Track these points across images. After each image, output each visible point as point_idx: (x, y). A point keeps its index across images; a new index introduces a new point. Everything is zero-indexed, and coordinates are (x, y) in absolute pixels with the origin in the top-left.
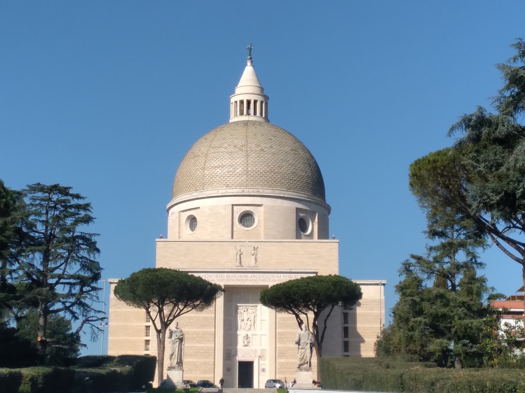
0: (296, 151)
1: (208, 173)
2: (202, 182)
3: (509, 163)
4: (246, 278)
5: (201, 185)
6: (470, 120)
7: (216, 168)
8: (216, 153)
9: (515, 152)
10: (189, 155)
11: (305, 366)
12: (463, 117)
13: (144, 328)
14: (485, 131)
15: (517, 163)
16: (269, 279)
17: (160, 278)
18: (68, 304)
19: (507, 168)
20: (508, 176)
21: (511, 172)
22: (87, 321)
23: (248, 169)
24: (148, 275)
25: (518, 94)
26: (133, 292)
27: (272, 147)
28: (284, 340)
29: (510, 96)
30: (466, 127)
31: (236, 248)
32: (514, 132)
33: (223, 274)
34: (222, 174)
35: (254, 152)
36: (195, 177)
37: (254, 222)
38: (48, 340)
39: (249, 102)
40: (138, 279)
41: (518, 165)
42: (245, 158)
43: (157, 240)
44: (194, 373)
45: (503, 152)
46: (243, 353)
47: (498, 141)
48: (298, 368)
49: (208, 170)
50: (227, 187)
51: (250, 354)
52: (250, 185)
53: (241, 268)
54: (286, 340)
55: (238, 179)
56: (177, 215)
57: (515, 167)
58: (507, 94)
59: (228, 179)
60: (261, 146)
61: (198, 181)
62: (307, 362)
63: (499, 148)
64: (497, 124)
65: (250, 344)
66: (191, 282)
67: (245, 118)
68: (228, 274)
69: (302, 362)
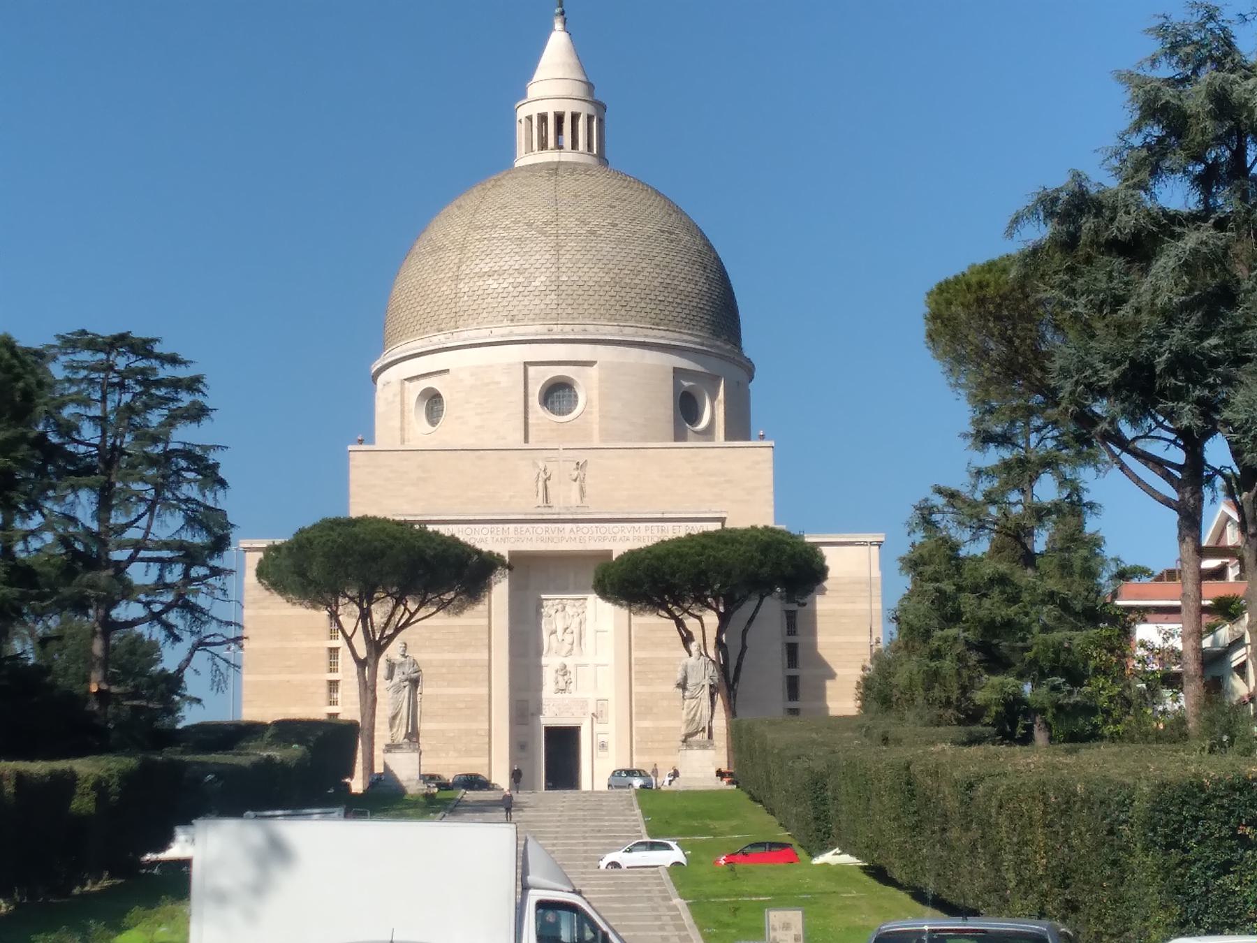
2: (454, 310)
3: (1139, 295)
4: (560, 535)
6: (1055, 200)
7: (485, 278)
8: (486, 242)
9: (1153, 271)
10: (421, 246)
11: (698, 737)
12: (1039, 194)
13: (325, 653)
14: (1088, 224)
15: (1158, 297)
16: (613, 535)
17: (363, 540)
18: (157, 608)
19: (1136, 308)
20: (1136, 326)
21: (1145, 317)
22: (201, 645)
23: (560, 279)
24: (334, 535)
25: (1160, 140)
26: (303, 574)
28: (650, 676)
29: (1143, 147)
30: (1046, 217)
31: (535, 465)
32: (1152, 227)
34: (500, 290)
35: (573, 237)
36: (435, 300)
37: (576, 402)
38: (114, 689)
39: (559, 118)
40: (311, 544)
41: (1158, 302)
42: (552, 252)
43: (350, 448)
45: (1127, 274)
46: (554, 708)
47: (1116, 247)
49: (466, 281)
50: (512, 320)
52: (564, 315)
53: (549, 510)
55: (537, 302)
56: (396, 388)
57: (1153, 304)
58: (1137, 141)
59: (515, 303)
62: (704, 728)
63: (1118, 263)
64: (1114, 209)
65: (572, 687)
66: (435, 549)
67: (550, 156)
68: (519, 526)
69: (692, 728)
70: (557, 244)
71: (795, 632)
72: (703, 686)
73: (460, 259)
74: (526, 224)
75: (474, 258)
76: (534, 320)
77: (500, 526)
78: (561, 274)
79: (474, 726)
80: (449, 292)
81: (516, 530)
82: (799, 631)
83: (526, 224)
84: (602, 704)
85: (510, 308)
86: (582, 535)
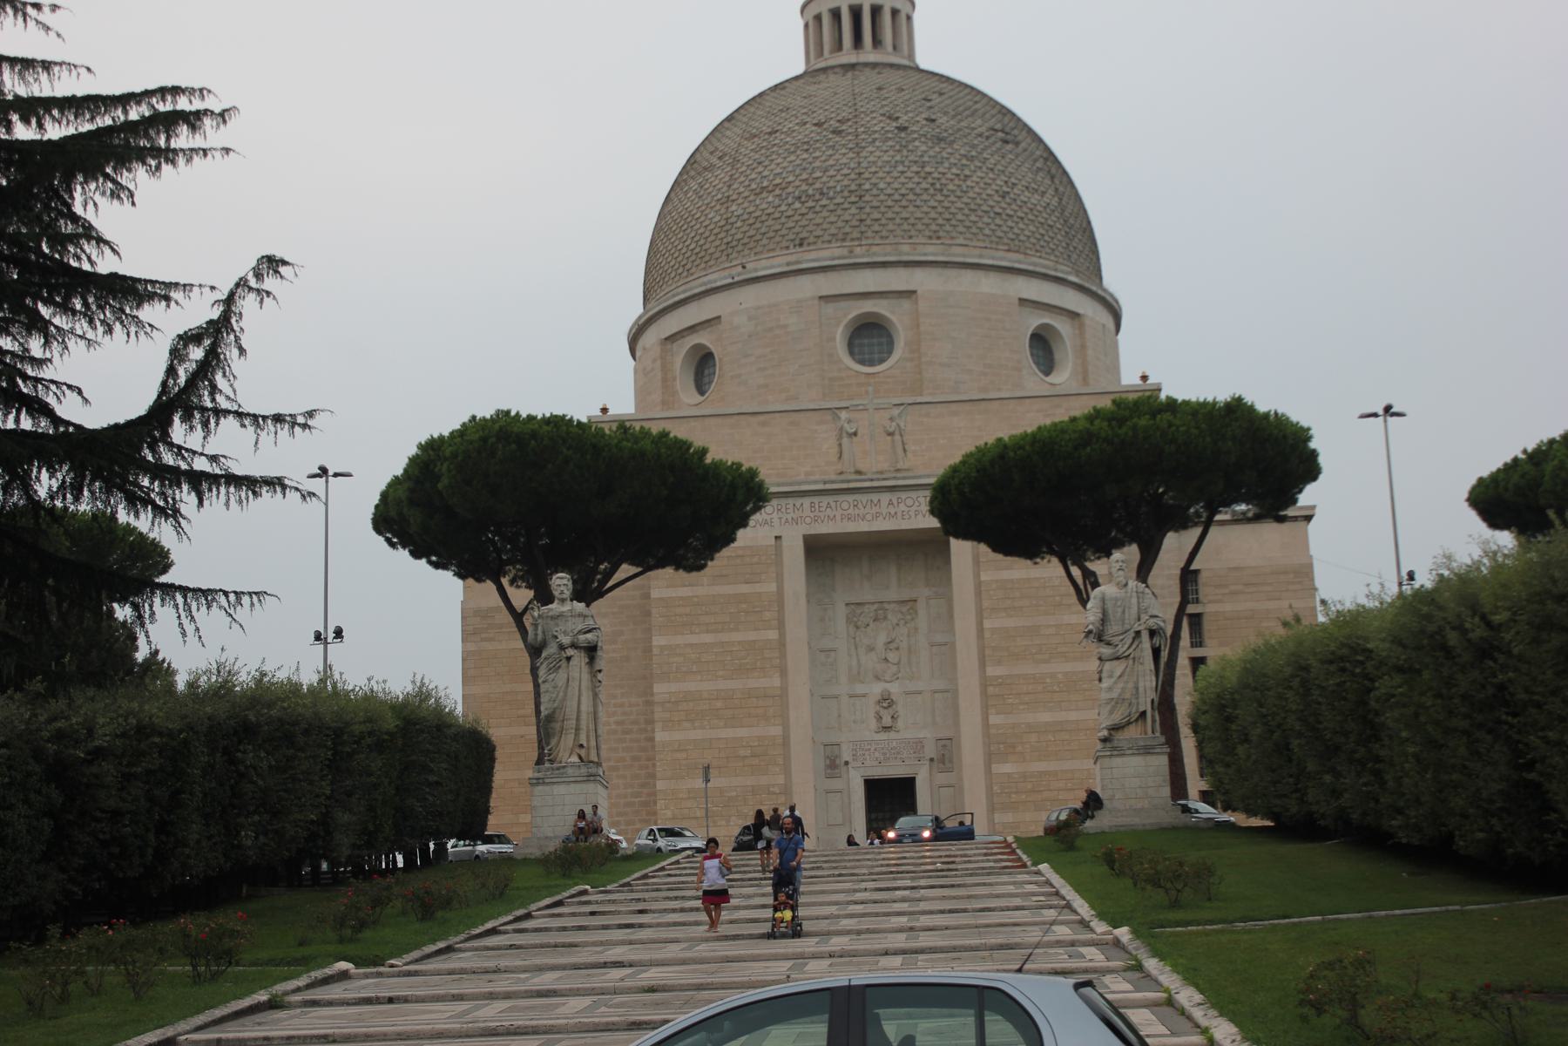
0: (1007, 133)
1: (740, 212)
2: (725, 241)
5: (723, 251)
7: (764, 195)
11: (1133, 732)
23: (863, 165)
27: (933, 121)
33: (798, 501)
34: (783, 208)
37: (890, 352)
39: (856, 13)
42: (851, 155)
44: (724, 823)
48: (1104, 740)
49: (740, 201)
50: (801, 245)
51: (899, 756)
52: (869, 234)
53: (858, 477)
54: (1017, 701)
59: (804, 222)
60: (897, 118)
61: (712, 238)
62: (1143, 714)
65: (900, 724)
67: (848, 56)
68: (816, 499)
69: (1117, 718)
70: (857, 144)
71: (1201, 642)
72: (1138, 633)
73: (731, 176)
74: (815, 125)
75: (748, 172)
76: (830, 242)
77: (791, 501)
78: (863, 181)
79: (764, 780)
80: (718, 218)
81: (812, 505)
82: (1207, 641)
83: (815, 125)
84: (944, 746)
85: (797, 229)
86: (906, 509)
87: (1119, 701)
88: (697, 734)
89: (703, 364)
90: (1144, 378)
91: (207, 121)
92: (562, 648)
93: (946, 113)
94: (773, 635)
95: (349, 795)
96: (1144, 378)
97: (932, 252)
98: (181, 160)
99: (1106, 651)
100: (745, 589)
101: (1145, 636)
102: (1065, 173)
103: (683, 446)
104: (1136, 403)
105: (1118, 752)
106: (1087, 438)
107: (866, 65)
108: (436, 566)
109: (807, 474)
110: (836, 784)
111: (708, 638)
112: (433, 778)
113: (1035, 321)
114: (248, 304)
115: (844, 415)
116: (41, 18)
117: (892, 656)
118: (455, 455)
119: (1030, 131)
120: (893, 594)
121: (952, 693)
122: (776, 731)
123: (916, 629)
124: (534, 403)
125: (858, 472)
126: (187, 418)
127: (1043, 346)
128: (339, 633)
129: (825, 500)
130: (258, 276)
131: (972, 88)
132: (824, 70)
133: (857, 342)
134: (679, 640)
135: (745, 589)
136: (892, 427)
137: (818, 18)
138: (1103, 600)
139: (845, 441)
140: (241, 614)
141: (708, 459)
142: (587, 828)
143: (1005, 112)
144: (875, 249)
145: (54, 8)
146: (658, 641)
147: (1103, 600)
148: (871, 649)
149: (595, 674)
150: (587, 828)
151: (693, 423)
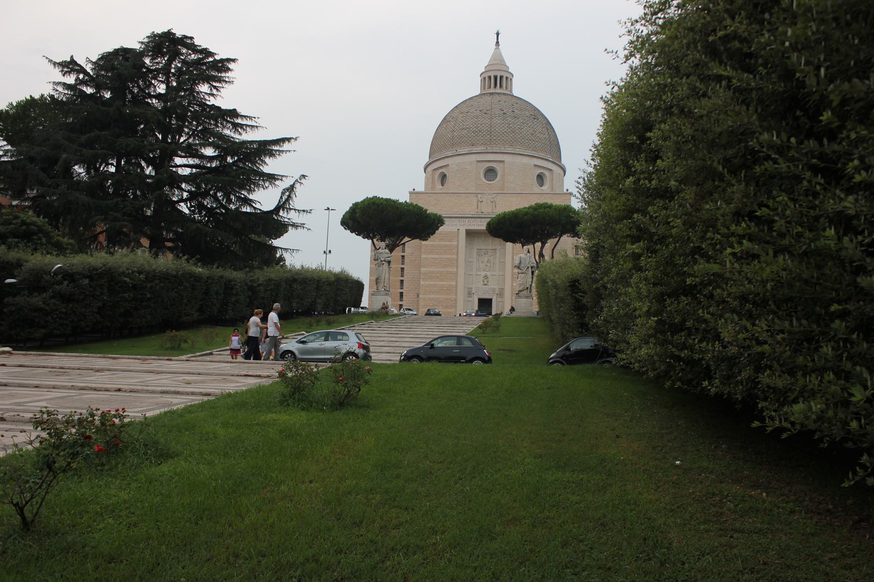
11: (525, 292)
13: (400, 270)
31: (477, 196)
39: (496, 78)
48: (517, 294)
56: (431, 173)
67: (492, 90)
69: (521, 288)
77: (463, 219)
79: (450, 297)
87: (521, 284)
88: (432, 283)
89: (444, 177)
90: (567, 190)
91: (292, 140)
92: (382, 261)
93: (517, 110)
94: (455, 256)
95: (321, 295)
96: (567, 190)
97: (510, 150)
98: (284, 153)
99: (520, 271)
100: (448, 243)
101: (530, 268)
102: (552, 127)
103: (421, 209)
104: (541, 205)
105: (520, 297)
106: (526, 214)
107: (497, 93)
108: (357, 235)
109: (470, 211)
110: (471, 299)
111: (437, 256)
112: (344, 292)
113: (539, 171)
114: (297, 185)
115: (479, 196)
116: (256, 120)
117: (489, 265)
118: (361, 208)
119: (543, 115)
120: (490, 247)
121: (504, 275)
122: (454, 283)
123: (496, 257)
124: (384, 194)
125: (482, 212)
126: (283, 210)
127: (540, 178)
128: (330, 252)
129: (472, 220)
130: (300, 179)
131: (527, 102)
132: (484, 94)
133: (487, 174)
134: (429, 256)
135: (448, 243)
136: (492, 200)
137: (485, 78)
138: (521, 258)
139: (479, 203)
140: (293, 254)
141: (428, 212)
142: (385, 307)
143: (536, 109)
144: (494, 148)
145: (258, 118)
146: (423, 256)
147: (521, 258)
148: (483, 262)
149: (390, 268)
150: (385, 307)
151: (438, 195)
